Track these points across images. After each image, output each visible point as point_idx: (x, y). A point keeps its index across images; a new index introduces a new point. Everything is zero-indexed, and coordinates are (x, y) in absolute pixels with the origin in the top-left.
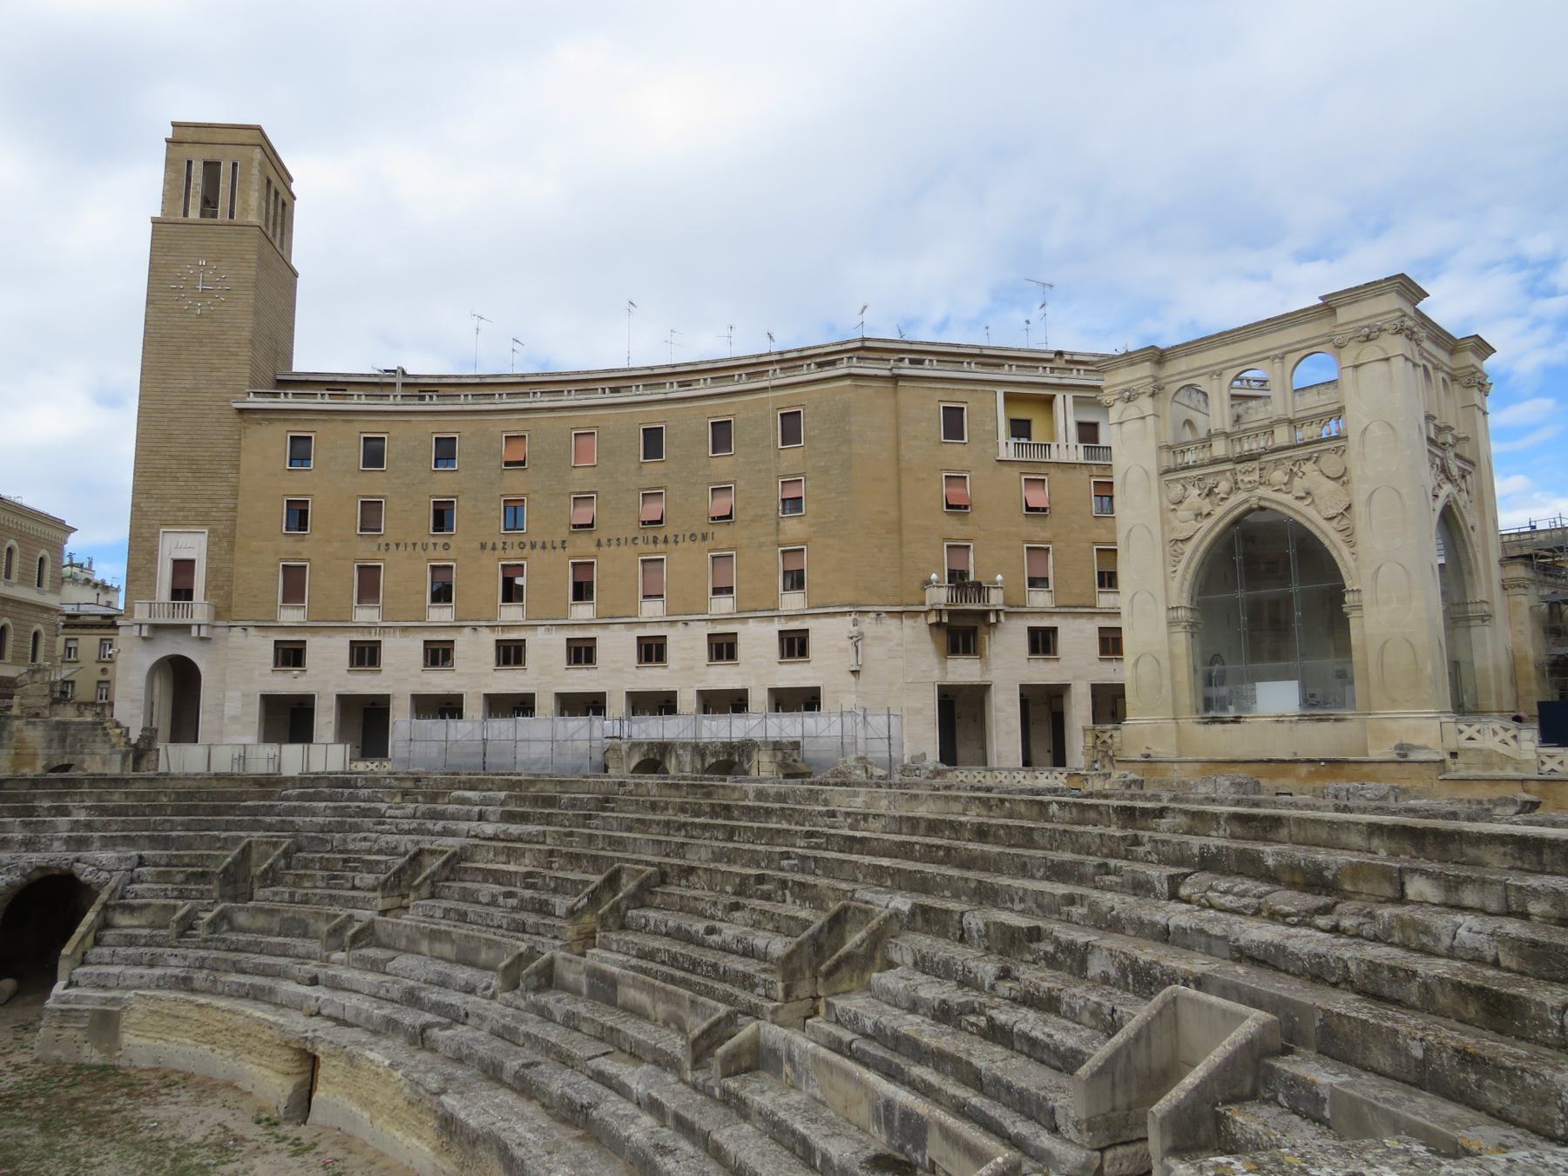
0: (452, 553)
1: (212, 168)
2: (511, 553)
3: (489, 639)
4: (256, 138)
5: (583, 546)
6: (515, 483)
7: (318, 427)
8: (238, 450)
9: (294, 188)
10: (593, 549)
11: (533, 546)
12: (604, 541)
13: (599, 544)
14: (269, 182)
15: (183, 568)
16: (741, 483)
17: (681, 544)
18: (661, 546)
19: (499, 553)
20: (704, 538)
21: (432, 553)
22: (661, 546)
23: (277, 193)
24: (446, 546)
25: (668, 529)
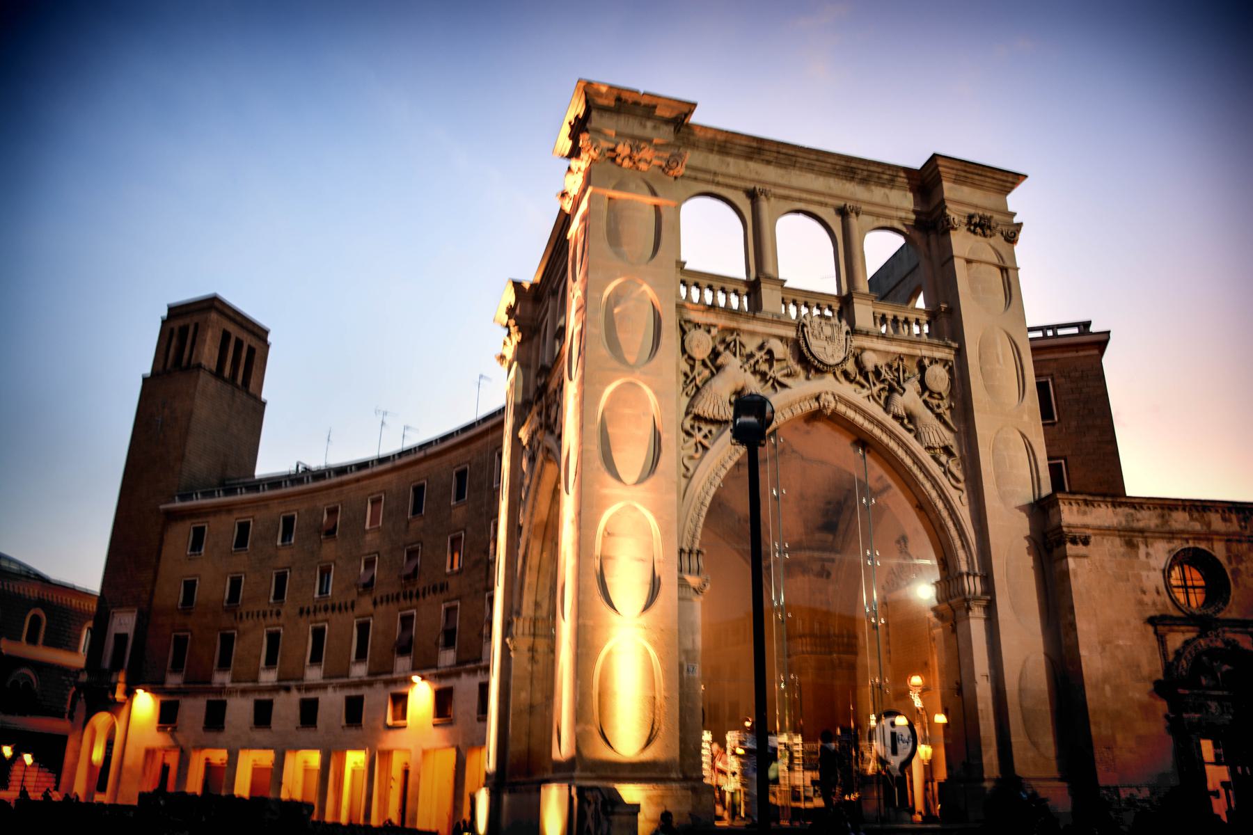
0: (281, 621)
1: (184, 330)
2: (320, 616)
3: (296, 697)
4: (213, 304)
5: (366, 604)
6: (329, 550)
7: (212, 520)
8: (162, 541)
9: (270, 339)
10: (371, 608)
11: (333, 609)
12: (378, 599)
13: (375, 603)
14: (226, 336)
15: (121, 639)
16: (469, 529)
17: (428, 598)
18: (414, 601)
19: (312, 617)
20: (442, 590)
21: (270, 620)
22: (414, 601)
23: (239, 344)
24: (278, 614)
25: (421, 584)
